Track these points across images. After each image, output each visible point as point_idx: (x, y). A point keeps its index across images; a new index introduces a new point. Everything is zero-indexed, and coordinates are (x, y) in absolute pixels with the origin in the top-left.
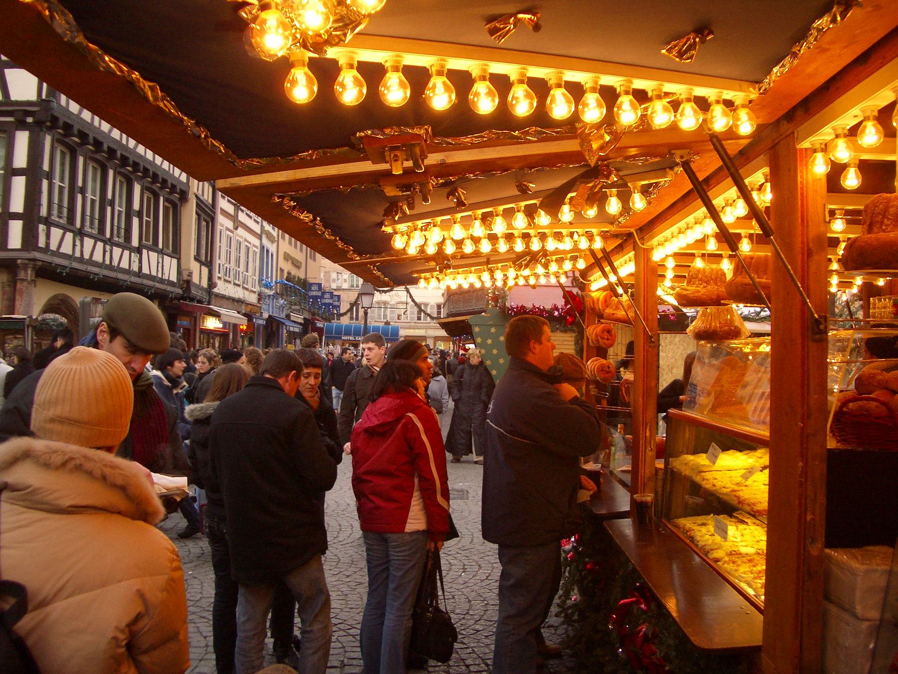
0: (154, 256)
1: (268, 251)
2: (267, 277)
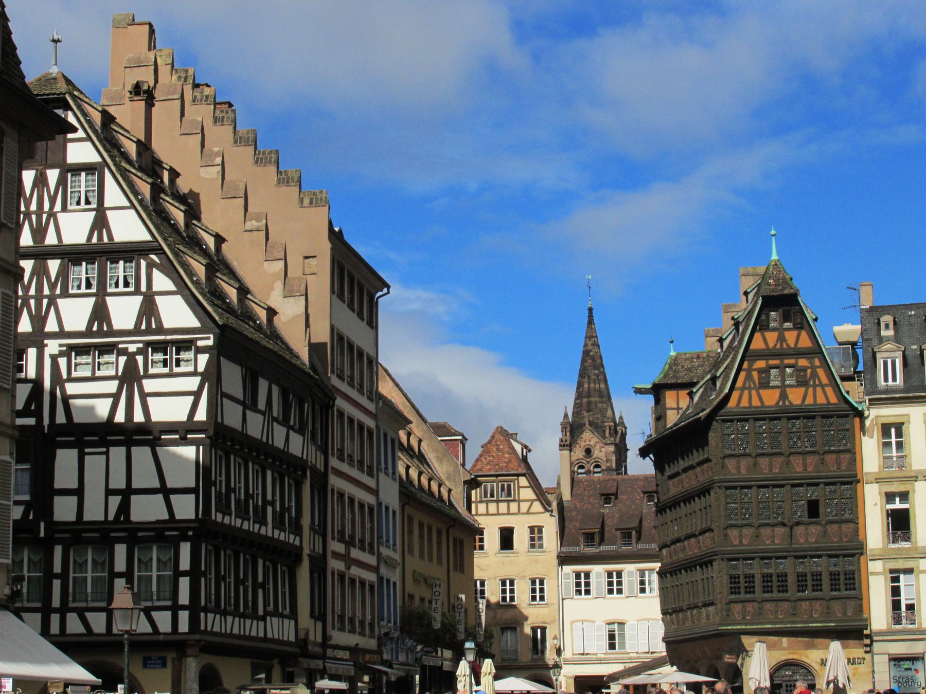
0: (275, 620)
1: (388, 581)
2: (389, 621)
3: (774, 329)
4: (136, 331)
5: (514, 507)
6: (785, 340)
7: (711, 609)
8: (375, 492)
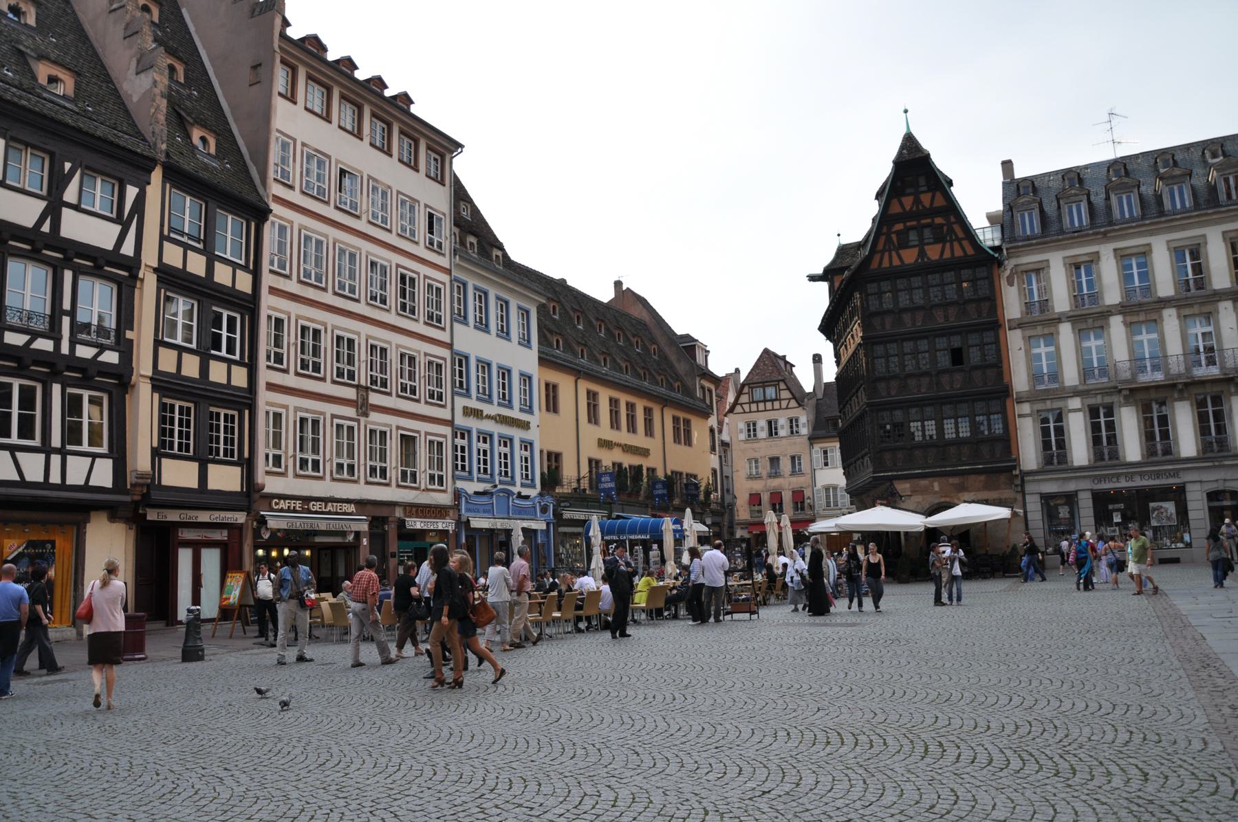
3: (909, 195)
5: (776, 404)
6: (921, 202)
7: (867, 459)
8: (450, 346)
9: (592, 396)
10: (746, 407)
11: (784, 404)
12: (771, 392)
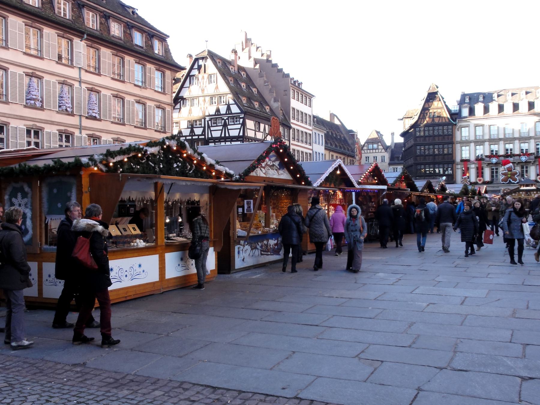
4: (226, 114)
8: (312, 150)
9: (332, 156)
10: (366, 151)
11: (380, 151)
12: (375, 146)
